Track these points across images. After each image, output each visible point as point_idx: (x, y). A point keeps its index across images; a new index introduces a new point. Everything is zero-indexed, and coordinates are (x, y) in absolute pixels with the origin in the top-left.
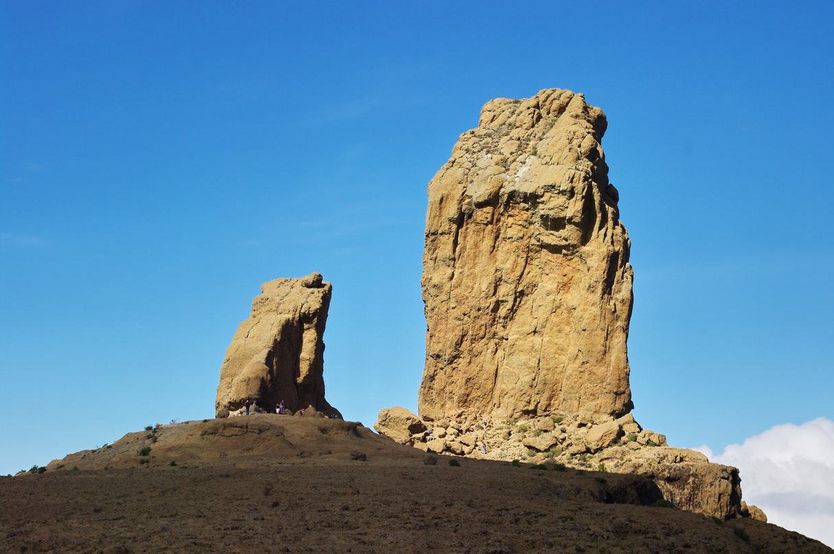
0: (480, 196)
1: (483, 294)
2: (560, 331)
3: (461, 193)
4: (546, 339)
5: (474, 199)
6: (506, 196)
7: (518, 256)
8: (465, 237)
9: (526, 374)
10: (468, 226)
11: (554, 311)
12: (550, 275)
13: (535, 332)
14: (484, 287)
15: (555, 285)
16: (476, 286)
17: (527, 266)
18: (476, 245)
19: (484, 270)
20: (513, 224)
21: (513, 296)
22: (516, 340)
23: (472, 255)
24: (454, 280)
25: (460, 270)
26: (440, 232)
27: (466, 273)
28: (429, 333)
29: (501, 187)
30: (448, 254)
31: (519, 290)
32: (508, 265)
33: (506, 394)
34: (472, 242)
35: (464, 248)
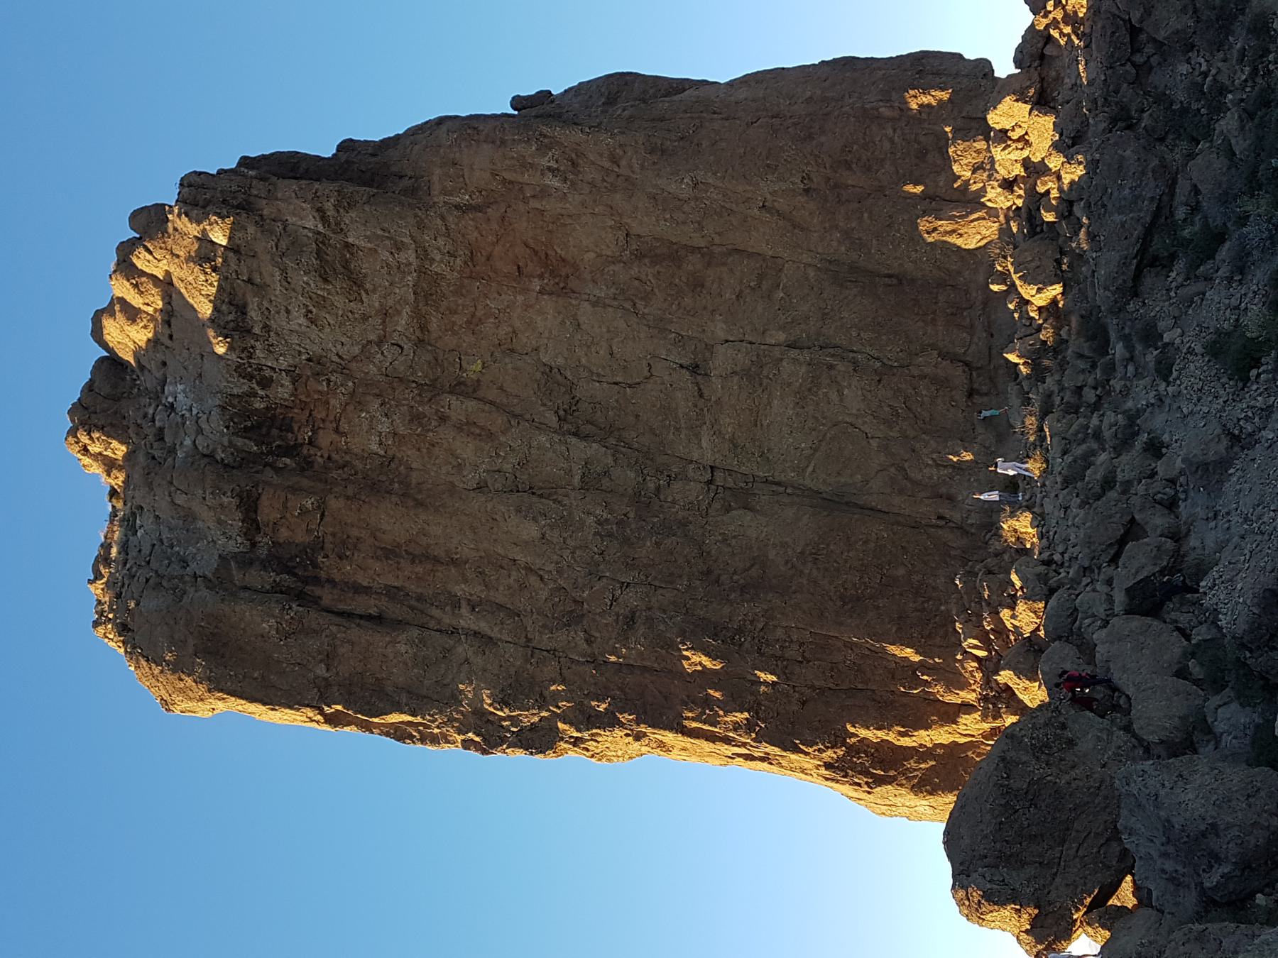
0: (219, 522)
1: (554, 536)
2: (697, 285)
3: (205, 593)
4: (719, 329)
5: (232, 547)
6: (239, 442)
7: (443, 419)
8: (358, 589)
9: (834, 396)
10: (323, 575)
11: (628, 305)
12: (517, 324)
13: (694, 369)
14: (530, 531)
15: (548, 303)
16: (521, 558)
17: (480, 394)
18: (389, 553)
19: (473, 529)
20: (337, 430)
21: (574, 440)
22: (718, 433)
23: (419, 569)
24: (495, 633)
25: (465, 611)
26: (321, 671)
27: (477, 590)
28: (669, 737)
29: (210, 456)
30: (402, 648)
31: (553, 420)
32: (467, 450)
33: (907, 477)
34: (377, 566)
35: (392, 593)
